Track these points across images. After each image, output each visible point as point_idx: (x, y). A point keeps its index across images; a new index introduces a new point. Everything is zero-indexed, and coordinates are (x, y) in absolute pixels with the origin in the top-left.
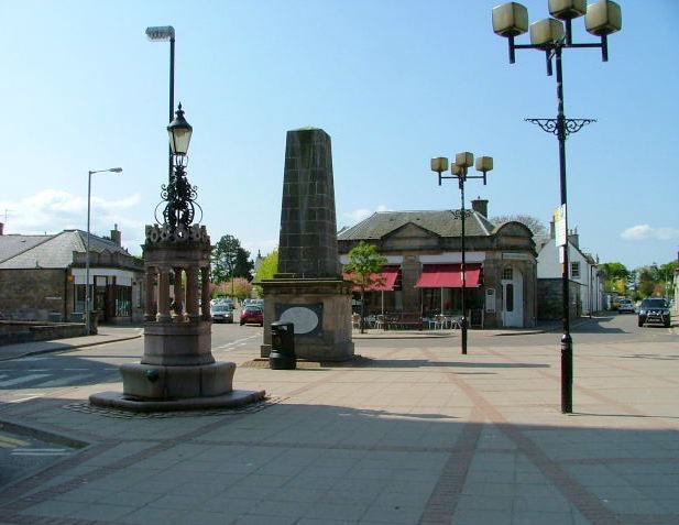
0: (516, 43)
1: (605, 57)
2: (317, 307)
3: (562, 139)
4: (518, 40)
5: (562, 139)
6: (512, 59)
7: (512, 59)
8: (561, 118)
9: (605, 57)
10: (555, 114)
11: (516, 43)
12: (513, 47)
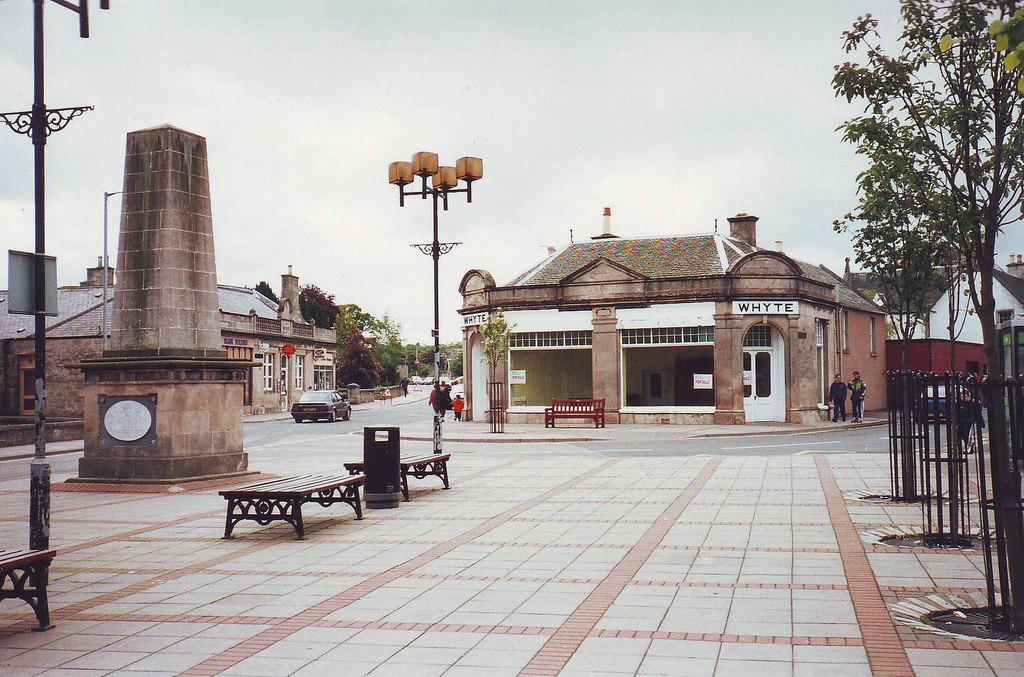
0: (405, 191)
1: (469, 200)
2: (150, 401)
3: (436, 258)
4: (407, 188)
5: (436, 258)
6: (402, 205)
7: (402, 205)
8: (436, 242)
9: (469, 200)
10: (431, 241)
11: (405, 191)
12: (402, 194)
